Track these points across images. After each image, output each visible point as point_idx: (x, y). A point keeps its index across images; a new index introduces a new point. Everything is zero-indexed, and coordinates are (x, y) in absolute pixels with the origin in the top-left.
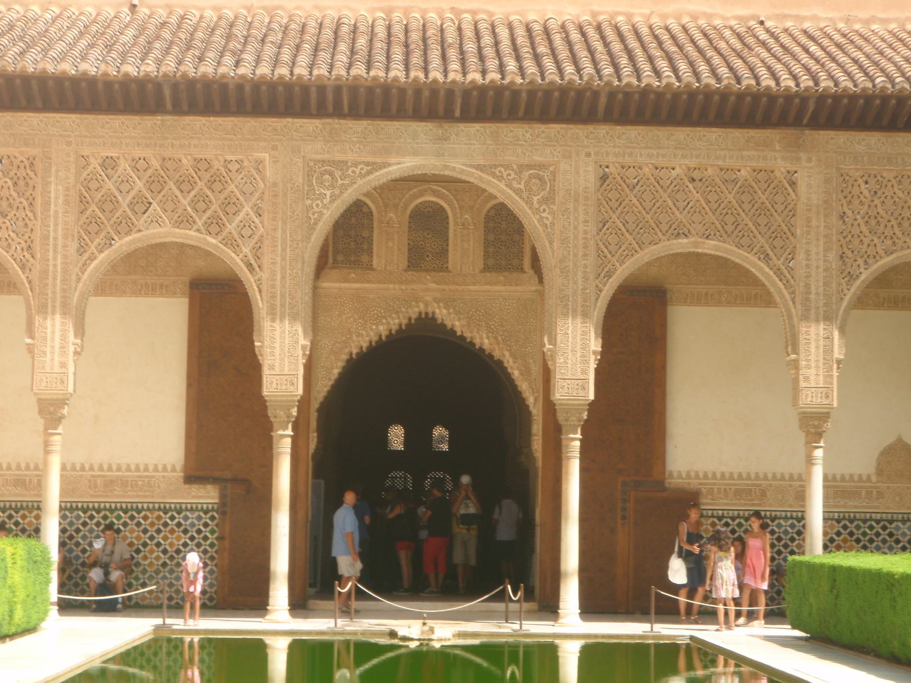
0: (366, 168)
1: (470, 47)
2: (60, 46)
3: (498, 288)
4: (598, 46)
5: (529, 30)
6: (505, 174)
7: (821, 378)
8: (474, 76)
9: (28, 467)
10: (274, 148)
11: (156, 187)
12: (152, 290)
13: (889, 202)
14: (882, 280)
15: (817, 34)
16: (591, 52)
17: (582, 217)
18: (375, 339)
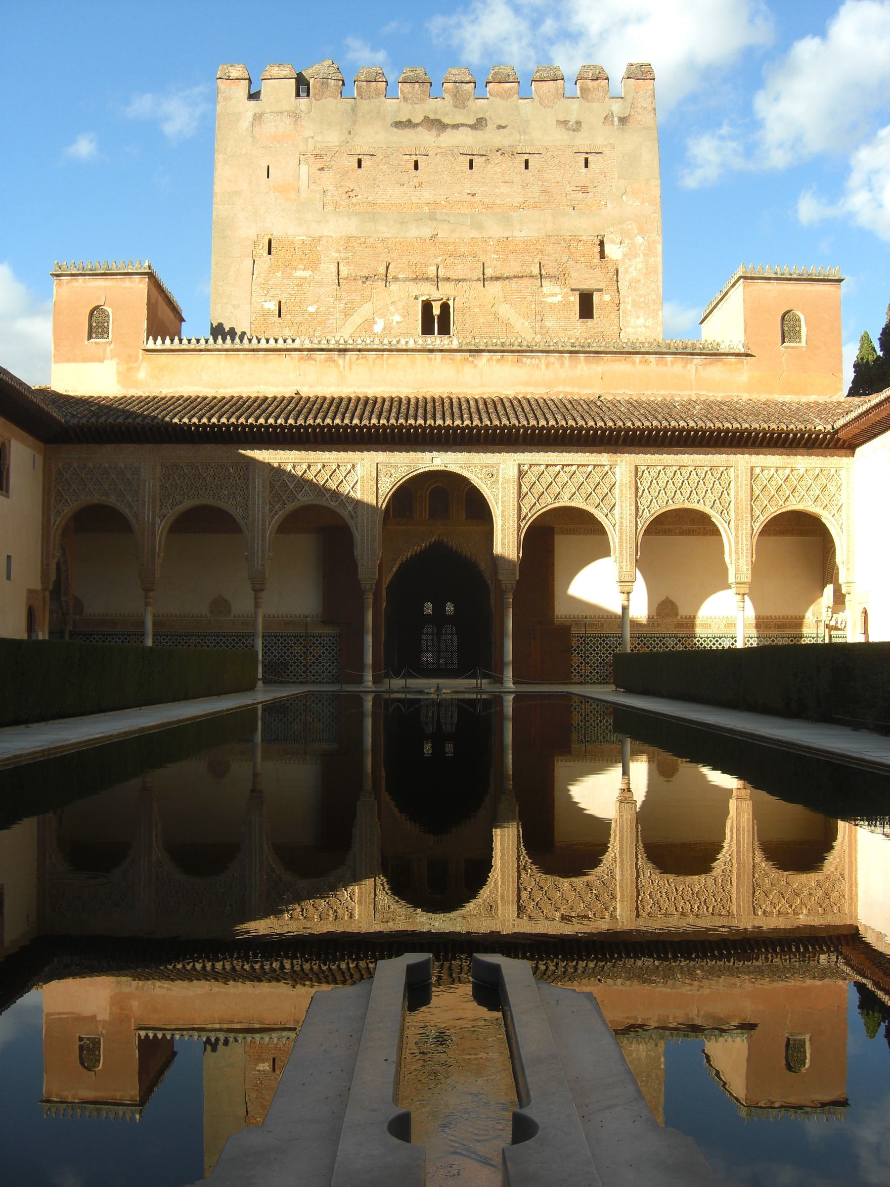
0: (407, 468)
1: (456, 410)
5: (485, 403)
6: (474, 470)
8: (458, 422)
9: (248, 617)
10: (362, 459)
17: (511, 492)
18: (414, 553)
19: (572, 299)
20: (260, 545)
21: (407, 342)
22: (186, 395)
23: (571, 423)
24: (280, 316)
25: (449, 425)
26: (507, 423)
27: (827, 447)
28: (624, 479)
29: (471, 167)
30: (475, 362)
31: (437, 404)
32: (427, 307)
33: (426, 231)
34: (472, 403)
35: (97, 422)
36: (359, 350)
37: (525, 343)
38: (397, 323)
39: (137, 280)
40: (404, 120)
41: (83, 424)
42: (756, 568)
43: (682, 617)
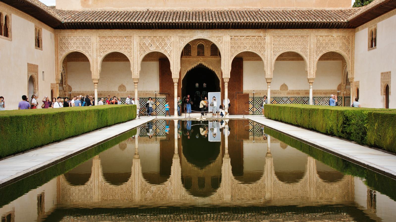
1: (207, 16)
2: (135, 17)
3: (213, 59)
4: (230, 15)
5: (218, 13)
7: (270, 74)
8: (208, 21)
9: (132, 92)
10: (173, 35)
11: (152, 42)
12: (152, 60)
13: (282, 42)
14: (281, 56)
15: (269, 12)
16: (229, 16)
18: (192, 68)
20: (136, 66)
22: (107, 11)
25: (204, 22)
26: (226, 21)
27: (345, 28)
28: (269, 41)
31: (200, 14)
34: (213, 13)
35: (74, 21)
41: (69, 22)
42: (317, 73)
43: (289, 91)
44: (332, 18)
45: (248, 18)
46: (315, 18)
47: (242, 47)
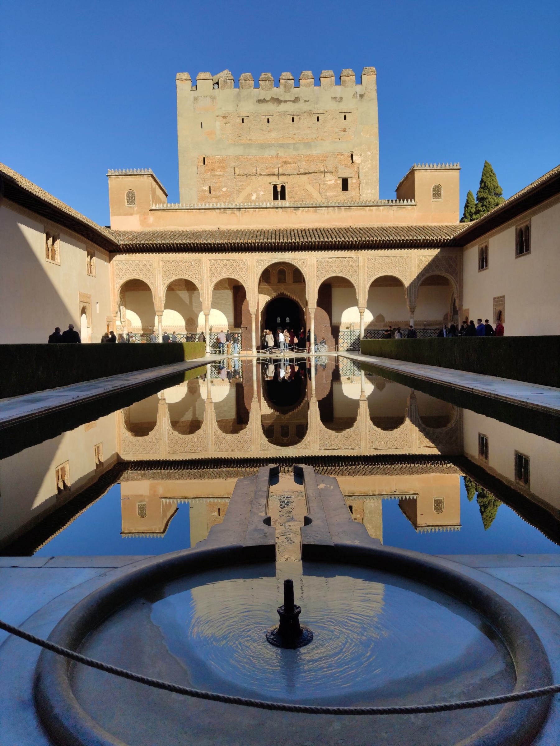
1: (289, 235)
5: (301, 231)
8: (289, 240)
15: (362, 229)
17: (313, 269)
19: (339, 182)
21: (266, 204)
23: (339, 239)
24: (210, 193)
27: (451, 246)
29: (293, 121)
30: (297, 213)
32: (275, 187)
33: (273, 152)
34: (296, 232)
36: (246, 208)
37: (318, 204)
38: (262, 195)
39: (146, 178)
40: (262, 99)
44: (437, 234)
45: (337, 237)
46: (417, 235)
47: (330, 271)
